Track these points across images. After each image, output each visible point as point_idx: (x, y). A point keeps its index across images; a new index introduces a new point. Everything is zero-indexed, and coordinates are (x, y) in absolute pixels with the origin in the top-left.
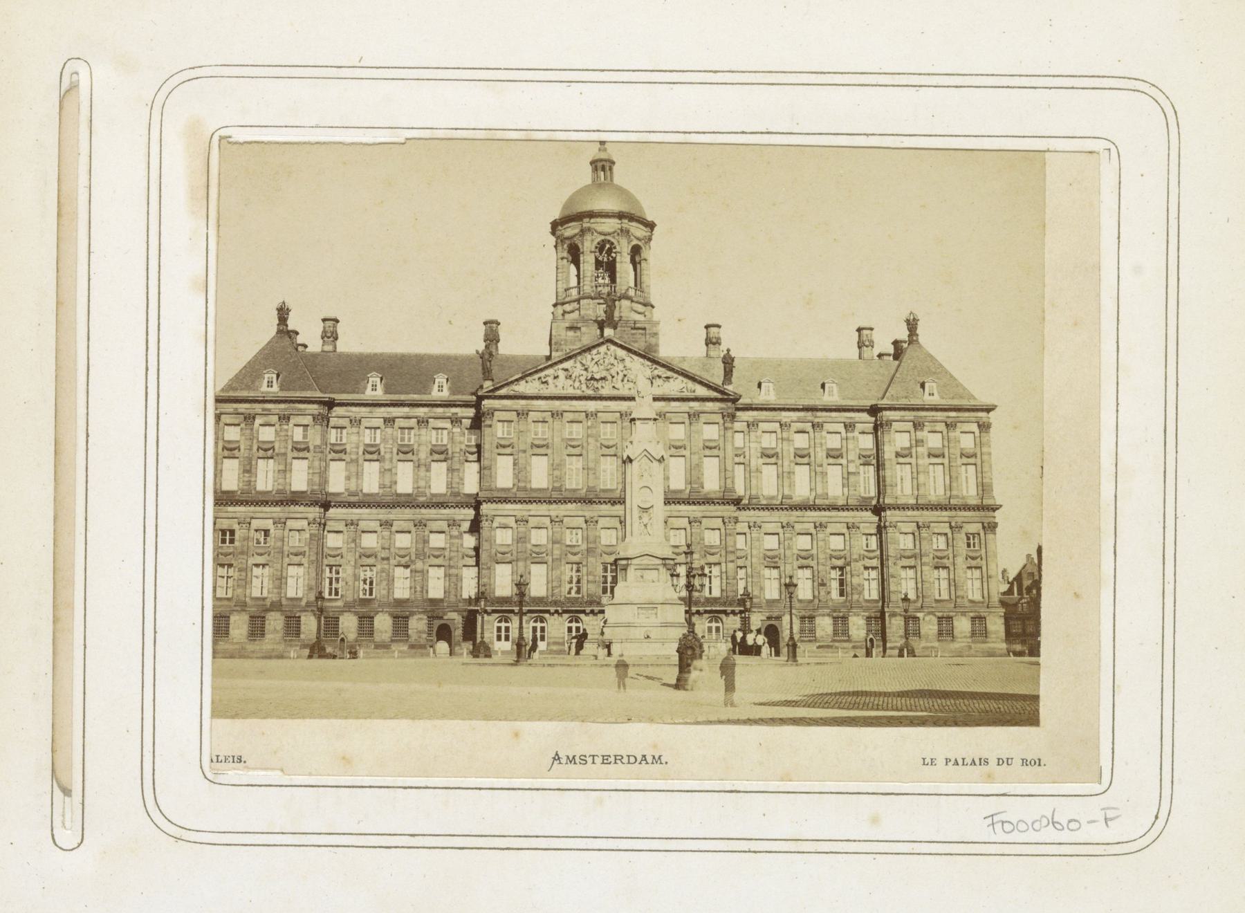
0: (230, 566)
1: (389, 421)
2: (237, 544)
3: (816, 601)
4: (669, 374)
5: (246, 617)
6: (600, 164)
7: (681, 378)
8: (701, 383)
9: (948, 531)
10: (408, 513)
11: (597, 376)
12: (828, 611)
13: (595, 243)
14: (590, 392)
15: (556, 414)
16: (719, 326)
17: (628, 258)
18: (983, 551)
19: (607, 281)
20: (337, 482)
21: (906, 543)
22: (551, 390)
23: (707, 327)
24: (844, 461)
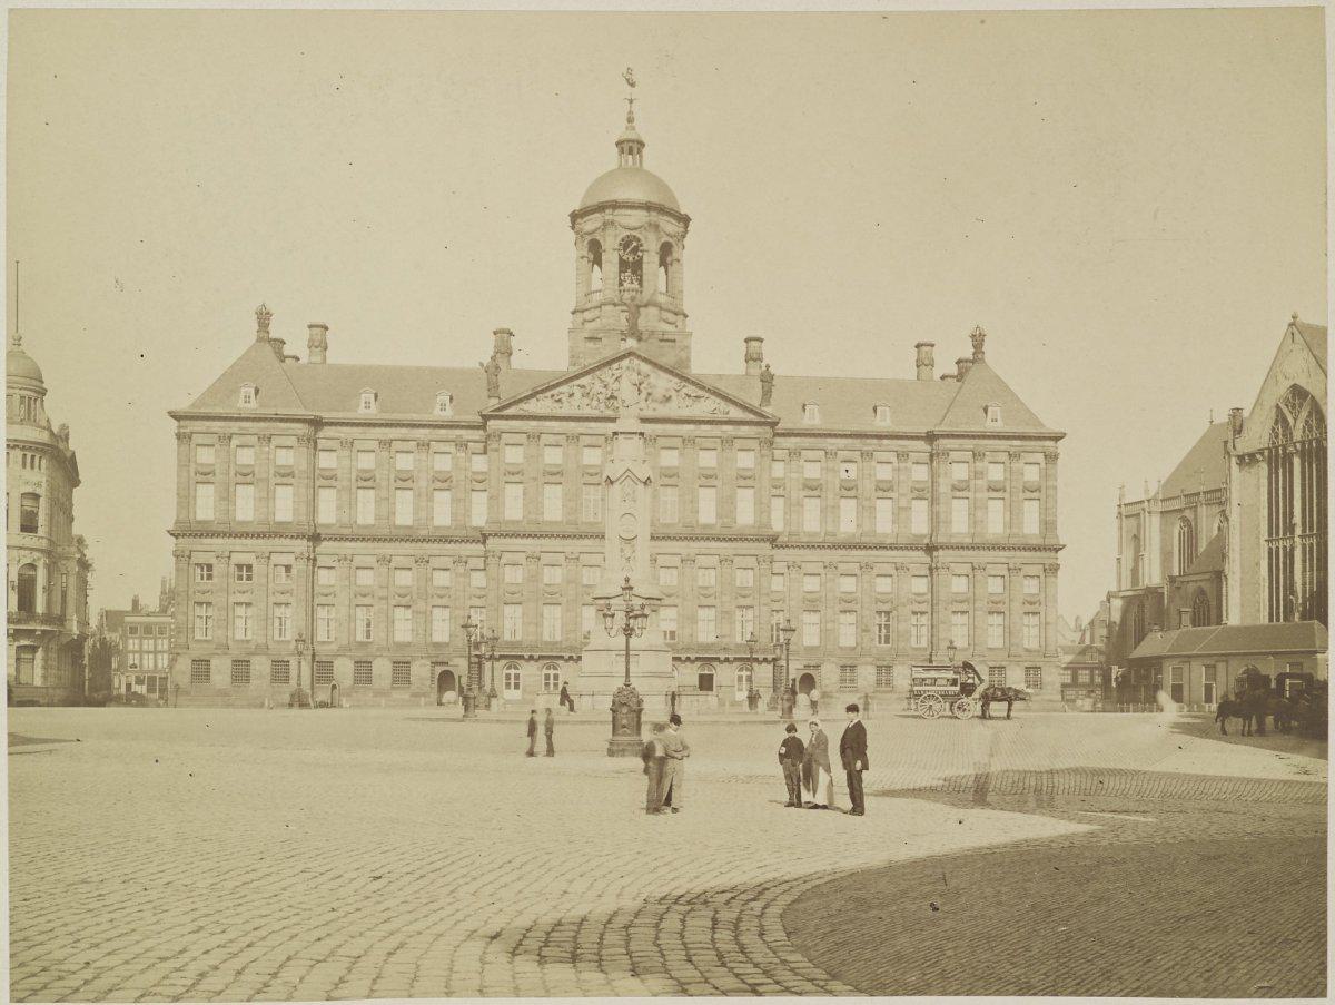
1: (386, 444)
2: (215, 580)
3: (859, 647)
4: (700, 393)
6: (626, 147)
7: (713, 397)
8: (734, 403)
9: (1005, 573)
10: (409, 548)
12: (870, 660)
13: (619, 239)
17: (657, 259)
18: (1043, 595)
19: (636, 285)
20: (328, 512)
21: (959, 585)
22: (565, 410)
23: (746, 341)
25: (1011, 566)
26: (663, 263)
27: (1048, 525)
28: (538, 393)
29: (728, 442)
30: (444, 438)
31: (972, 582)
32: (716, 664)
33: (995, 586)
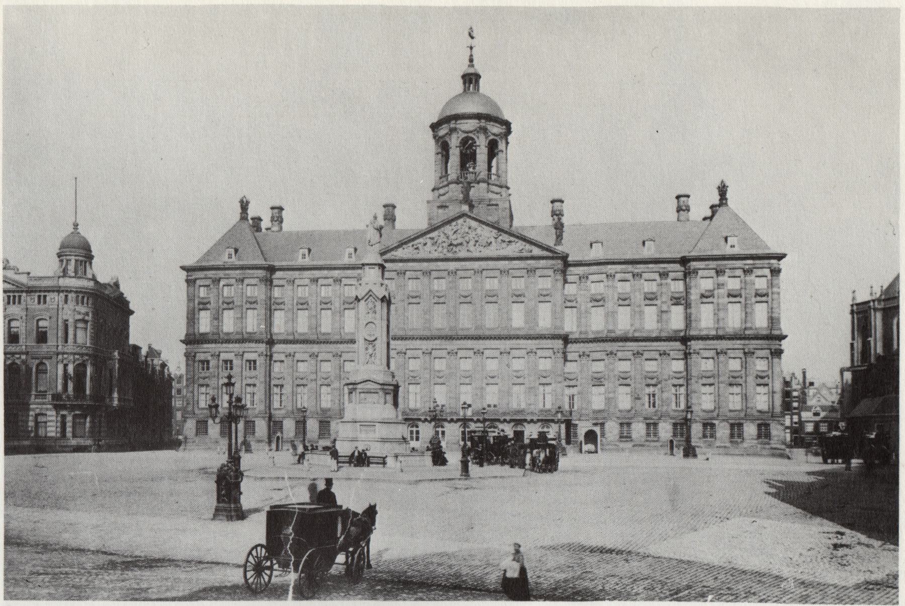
0: (207, 386)
1: (315, 280)
4: (512, 239)
7: (520, 242)
9: (742, 355)
11: (455, 242)
14: (450, 255)
15: (427, 273)
16: (562, 201)
22: (422, 255)
25: (746, 350)
28: (402, 244)
29: (531, 271)
32: (525, 424)
33: (735, 365)
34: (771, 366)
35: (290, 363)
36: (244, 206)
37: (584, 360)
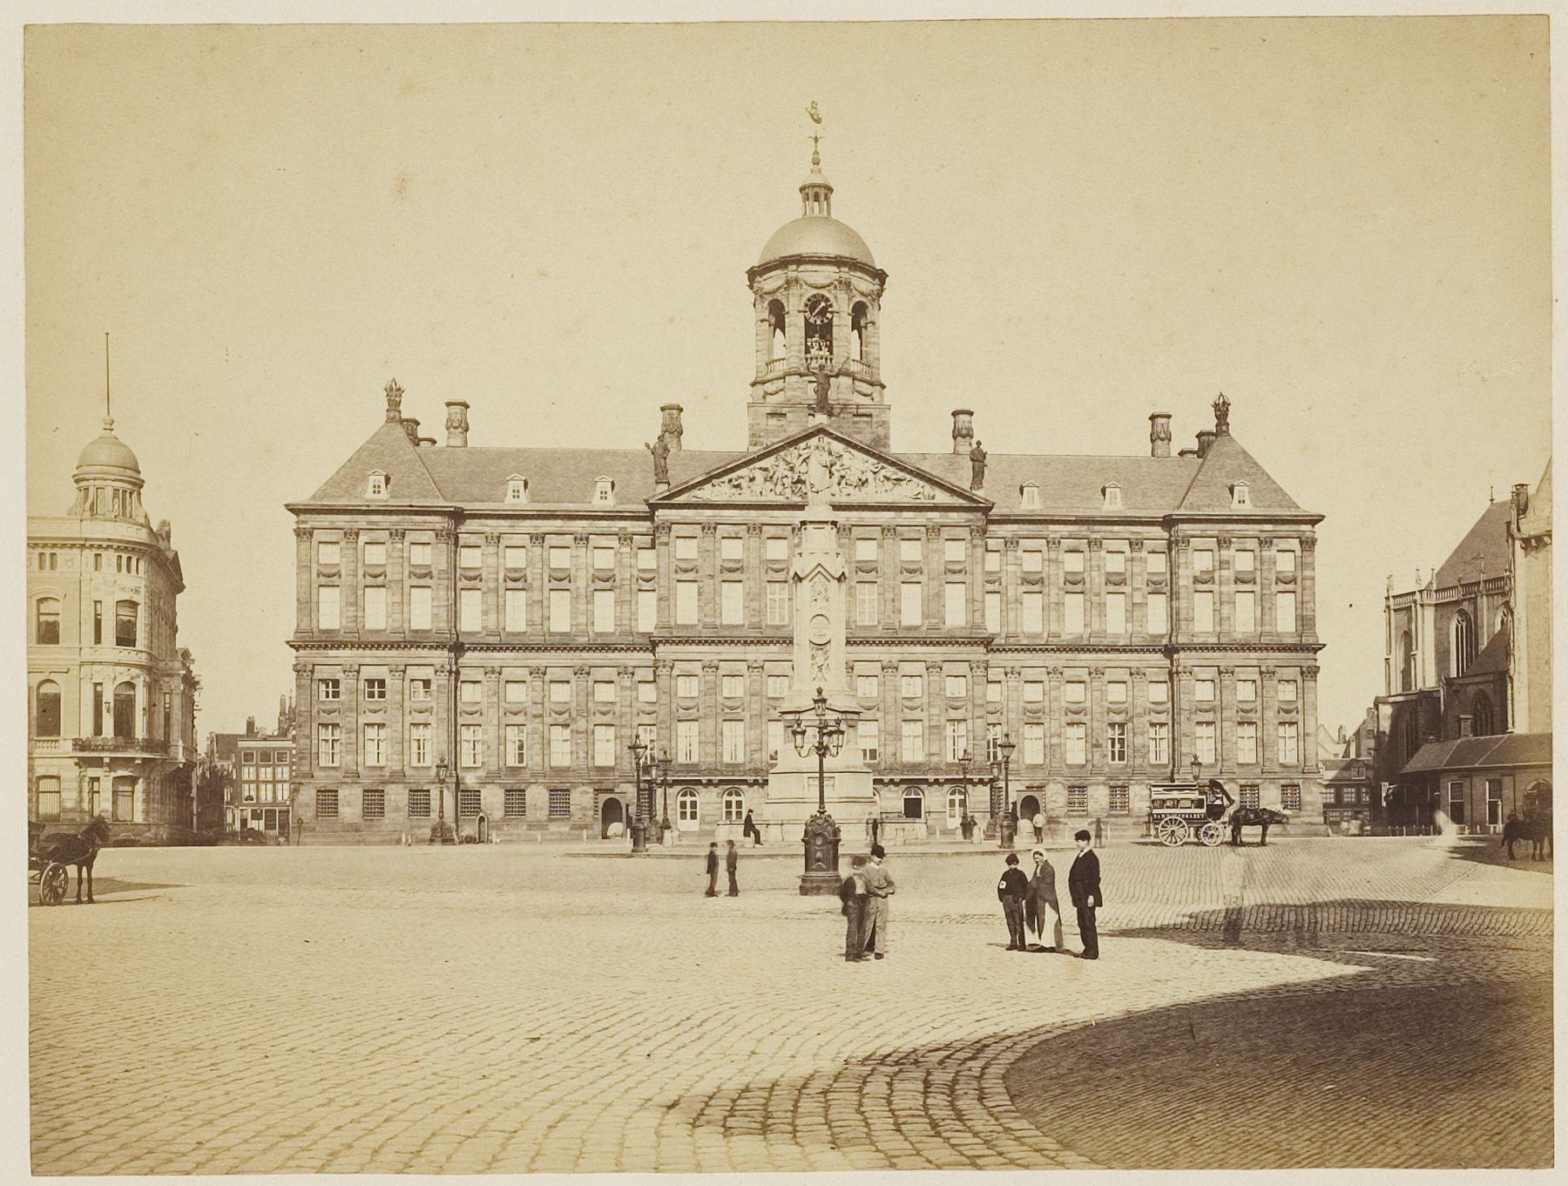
0: (335, 726)
1: (538, 538)
4: (901, 475)
5: (359, 791)
6: (811, 192)
8: (941, 486)
9: (1257, 677)
12: (1102, 779)
13: (805, 299)
15: (757, 528)
18: (1300, 702)
20: (472, 619)
22: (746, 497)
24: (1127, 589)
26: (856, 326)
27: (1305, 621)
29: (934, 530)
30: (606, 530)
31: (1220, 688)
32: (923, 787)
33: (1246, 692)
34: (1302, 693)
35: (493, 685)
36: (394, 396)
37: (1013, 681)
